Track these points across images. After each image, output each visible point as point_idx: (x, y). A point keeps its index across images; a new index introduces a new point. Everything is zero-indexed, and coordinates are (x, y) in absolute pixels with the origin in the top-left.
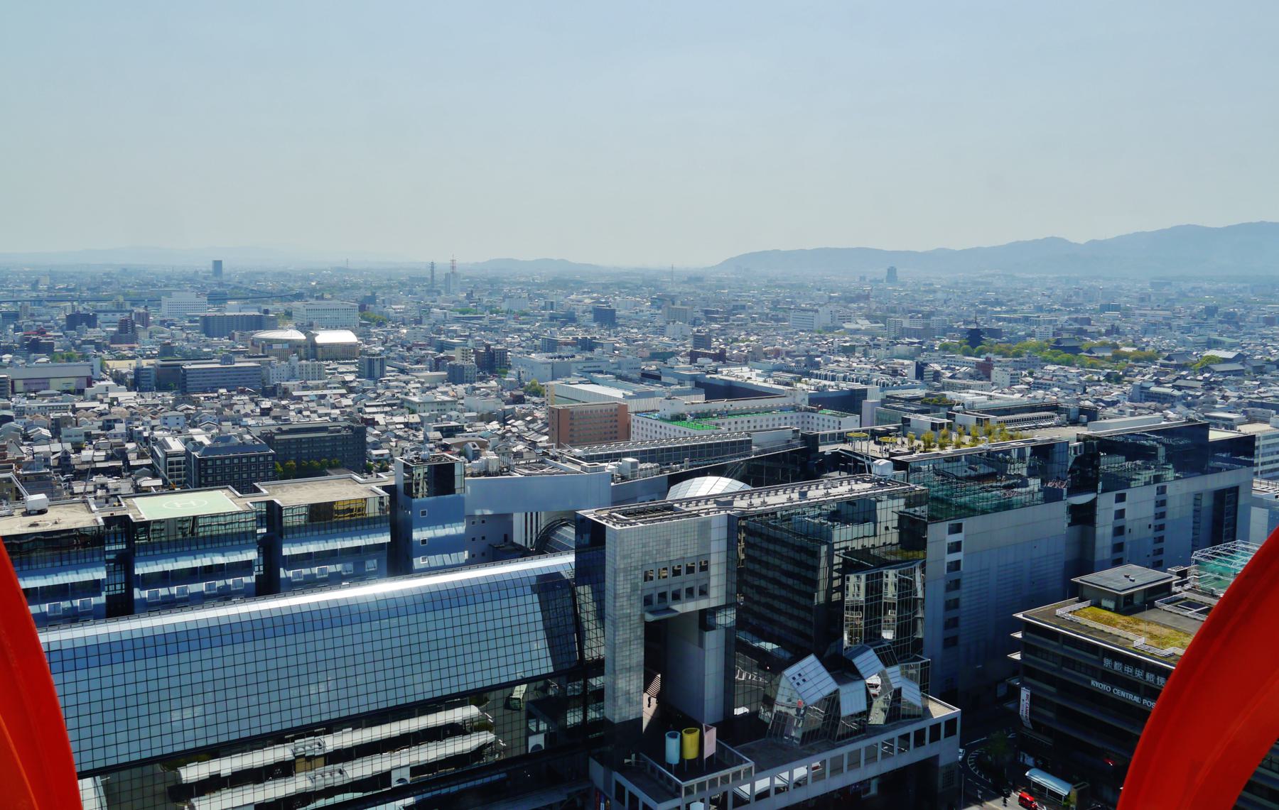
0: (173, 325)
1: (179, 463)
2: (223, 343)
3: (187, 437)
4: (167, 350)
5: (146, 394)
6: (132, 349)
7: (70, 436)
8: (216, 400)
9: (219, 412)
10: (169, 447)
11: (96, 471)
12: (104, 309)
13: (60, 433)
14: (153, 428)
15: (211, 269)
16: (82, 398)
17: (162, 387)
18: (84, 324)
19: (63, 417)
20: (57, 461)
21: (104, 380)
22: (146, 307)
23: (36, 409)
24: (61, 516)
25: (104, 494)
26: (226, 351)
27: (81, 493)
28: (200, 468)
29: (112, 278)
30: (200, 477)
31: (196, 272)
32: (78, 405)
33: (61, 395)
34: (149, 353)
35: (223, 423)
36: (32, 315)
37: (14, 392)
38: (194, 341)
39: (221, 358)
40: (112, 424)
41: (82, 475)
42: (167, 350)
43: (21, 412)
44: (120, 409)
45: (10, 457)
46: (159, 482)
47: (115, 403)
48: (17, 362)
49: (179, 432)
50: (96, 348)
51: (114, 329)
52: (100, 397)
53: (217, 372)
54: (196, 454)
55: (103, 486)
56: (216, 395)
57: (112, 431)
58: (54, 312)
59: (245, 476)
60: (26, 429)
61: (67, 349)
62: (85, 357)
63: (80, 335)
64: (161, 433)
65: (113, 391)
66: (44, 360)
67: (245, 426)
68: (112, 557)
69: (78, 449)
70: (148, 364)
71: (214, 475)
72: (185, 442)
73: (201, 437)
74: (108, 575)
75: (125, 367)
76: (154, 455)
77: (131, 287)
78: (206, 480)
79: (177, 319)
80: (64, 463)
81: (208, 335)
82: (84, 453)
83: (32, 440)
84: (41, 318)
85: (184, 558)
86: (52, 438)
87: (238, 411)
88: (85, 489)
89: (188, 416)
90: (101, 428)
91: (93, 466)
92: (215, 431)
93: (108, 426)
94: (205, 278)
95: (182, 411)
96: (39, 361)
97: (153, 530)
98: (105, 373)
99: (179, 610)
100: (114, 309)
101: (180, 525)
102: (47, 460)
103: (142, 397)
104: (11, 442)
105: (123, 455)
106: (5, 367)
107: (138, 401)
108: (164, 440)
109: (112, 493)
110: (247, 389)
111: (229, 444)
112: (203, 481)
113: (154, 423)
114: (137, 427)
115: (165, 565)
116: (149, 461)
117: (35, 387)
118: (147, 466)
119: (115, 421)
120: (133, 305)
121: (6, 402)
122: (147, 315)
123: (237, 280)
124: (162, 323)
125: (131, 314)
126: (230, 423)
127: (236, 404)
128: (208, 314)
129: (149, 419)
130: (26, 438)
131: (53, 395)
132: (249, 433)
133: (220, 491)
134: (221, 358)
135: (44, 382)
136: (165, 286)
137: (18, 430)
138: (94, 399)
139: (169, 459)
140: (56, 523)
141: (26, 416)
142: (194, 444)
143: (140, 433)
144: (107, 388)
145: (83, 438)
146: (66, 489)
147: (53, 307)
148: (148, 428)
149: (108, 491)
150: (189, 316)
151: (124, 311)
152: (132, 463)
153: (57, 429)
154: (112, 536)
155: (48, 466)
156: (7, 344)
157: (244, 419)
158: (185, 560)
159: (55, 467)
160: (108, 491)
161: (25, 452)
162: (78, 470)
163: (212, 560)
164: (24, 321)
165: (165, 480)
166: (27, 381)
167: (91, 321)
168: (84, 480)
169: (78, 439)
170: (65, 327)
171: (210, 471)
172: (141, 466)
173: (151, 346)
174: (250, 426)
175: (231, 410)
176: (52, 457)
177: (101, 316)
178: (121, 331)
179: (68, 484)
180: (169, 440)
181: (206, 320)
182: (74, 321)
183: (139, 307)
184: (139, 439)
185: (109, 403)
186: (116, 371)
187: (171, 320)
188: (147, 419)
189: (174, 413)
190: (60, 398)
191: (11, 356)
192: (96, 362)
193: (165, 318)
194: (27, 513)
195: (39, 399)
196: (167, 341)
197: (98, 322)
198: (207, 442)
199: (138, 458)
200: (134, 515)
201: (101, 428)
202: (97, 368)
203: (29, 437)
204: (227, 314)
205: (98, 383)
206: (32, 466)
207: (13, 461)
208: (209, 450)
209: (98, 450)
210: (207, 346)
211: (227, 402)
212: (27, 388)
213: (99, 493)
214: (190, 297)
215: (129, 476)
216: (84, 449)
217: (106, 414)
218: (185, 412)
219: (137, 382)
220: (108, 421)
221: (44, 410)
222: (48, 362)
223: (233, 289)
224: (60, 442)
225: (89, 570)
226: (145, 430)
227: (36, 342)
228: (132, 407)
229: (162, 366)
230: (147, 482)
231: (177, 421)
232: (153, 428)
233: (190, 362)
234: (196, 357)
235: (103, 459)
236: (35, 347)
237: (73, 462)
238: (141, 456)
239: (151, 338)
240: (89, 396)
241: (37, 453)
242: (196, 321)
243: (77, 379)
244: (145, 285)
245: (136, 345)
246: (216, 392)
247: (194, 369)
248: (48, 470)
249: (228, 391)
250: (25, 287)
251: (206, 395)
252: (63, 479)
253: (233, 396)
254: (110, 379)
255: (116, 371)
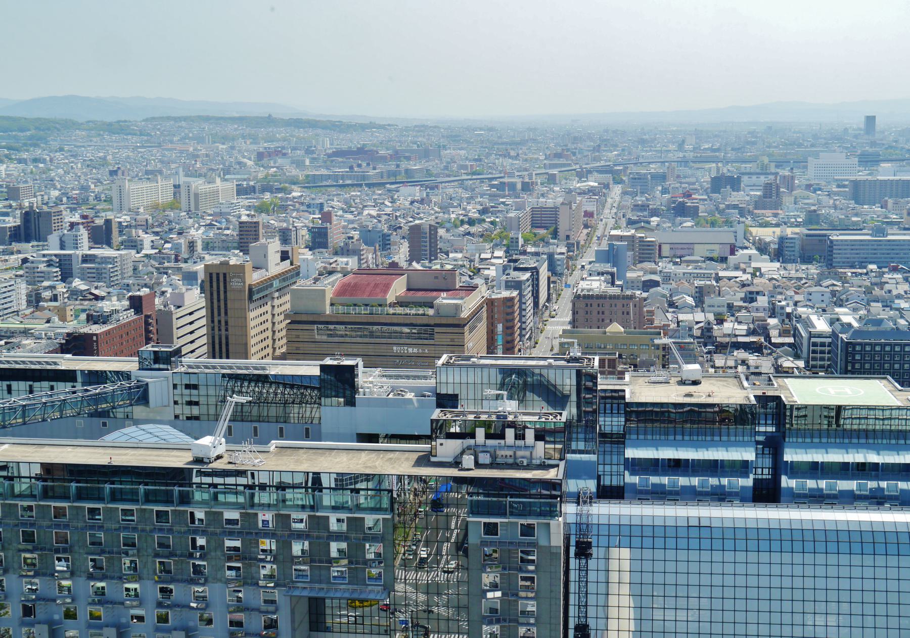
0: (820, 189)
1: (823, 345)
2: (874, 212)
3: (833, 316)
4: (812, 218)
5: (789, 266)
6: (775, 215)
7: (713, 306)
8: (864, 277)
9: (868, 291)
10: (814, 327)
11: (737, 346)
12: (748, 170)
13: (703, 302)
14: (796, 304)
15: (862, 126)
16: (725, 266)
17: (806, 259)
18: (728, 187)
19: (706, 285)
20: (700, 331)
21: (746, 248)
22: (792, 169)
23: (682, 275)
24: (714, 388)
25: (745, 370)
26: (878, 221)
27: (722, 368)
28: (847, 353)
29: (756, 137)
30: (847, 362)
31: (846, 130)
32: (721, 274)
33: (704, 262)
34: (793, 220)
35: (872, 304)
36: (678, 176)
37: (660, 257)
38: (841, 209)
39: (872, 229)
40: (754, 296)
41: (721, 348)
42: (812, 218)
43: (667, 278)
44: (763, 280)
45: (657, 323)
46: (801, 364)
47: (758, 274)
48: (664, 226)
49: (824, 310)
50: (739, 214)
51: (758, 193)
52: (743, 266)
53: (867, 245)
54: (844, 336)
55: (744, 362)
56: (865, 271)
57: (754, 304)
58: (699, 173)
59: (897, 366)
60: (671, 295)
61: (711, 213)
62: (728, 223)
63: (724, 199)
64: (805, 309)
65: (757, 261)
66: (689, 224)
67: (897, 309)
68: (761, 438)
69: (720, 321)
70: (793, 233)
71: (862, 362)
72: (832, 323)
73: (847, 317)
74: (756, 457)
75: (769, 235)
76: (796, 334)
77: (776, 147)
78: (853, 367)
79: (824, 183)
80: (707, 335)
81: (857, 203)
82: (726, 325)
83: (677, 307)
84: (687, 180)
85: (836, 450)
86: (696, 307)
87: (890, 291)
88: (725, 363)
89: (833, 293)
90: (744, 300)
91: (734, 340)
92: (863, 312)
93: (750, 298)
94: (856, 136)
95: (828, 287)
96: (685, 225)
97: (797, 417)
98: (748, 240)
99: (796, 506)
100: (758, 171)
101: (826, 414)
102: (690, 329)
103: (785, 269)
104: (658, 308)
105: (764, 331)
106: (652, 230)
107: (782, 273)
108: (808, 318)
109: (752, 370)
110: (901, 266)
111: (882, 328)
112: (849, 368)
113: (797, 298)
114: (780, 302)
115: (815, 455)
116: (791, 340)
117: (680, 254)
118: (789, 345)
119: (758, 293)
120: (777, 167)
121: (653, 265)
122: (793, 178)
123: (891, 138)
124: (808, 187)
125: (776, 177)
126: (880, 305)
127: (887, 283)
128: (859, 178)
129: (793, 293)
130: (672, 304)
131: (697, 262)
132: (902, 317)
133: (877, 381)
134: (872, 229)
135: (689, 247)
136: (812, 146)
137: (664, 296)
138: (737, 268)
139: (813, 340)
140: (709, 396)
141: (671, 281)
142: (842, 325)
143: (782, 308)
144: (750, 257)
145: (725, 309)
146: (707, 361)
147: (698, 169)
148: (791, 303)
149: (748, 368)
150: (837, 180)
151: (768, 174)
152: (773, 340)
153: (700, 296)
154: (763, 416)
155: (692, 336)
156: (655, 207)
157: (897, 301)
158: (837, 453)
159: (698, 338)
160: (748, 368)
161: (670, 319)
162: (719, 342)
163: (865, 457)
164: (671, 183)
165: (807, 362)
166: (672, 246)
167: (734, 183)
168: (725, 354)
169: (720, 310)
170: (709, 190)
171: (858, 357)
172: (783, 345)
173: (796, 213)
174: (903, 309)
175: (882, 289)
176: (696, 327)
177: (745, 179)
178: (765, 196)
179: (709, 356)
180: (814, 318)
181: (856, 184)
182: (719, 183)
183: (784, 169)
184: (782, 314)
185: (752, 274)
186: (760, 239)
187: (818, 184)
188: (790, 293)
189: (818, 288)
190: (703, 265)
191: (658, 219)
192: (740, 229)
193: (812, 182)
194: (682, 383)
195: (684, 265)
196: (813, 208)
197: (742, 185)
198: (856, 324)
199: (780, 336)
200: (786, 397)
201: (744, 300)
202: (740, 235)
203: (674, 304)
204: (880, 178)
205: (741, 252)
206: (677, 334)
207: (660, 328)
208: (858, 333)
209: (740, 323)
210: (856, 215)
211: (877, 280)
212: (673, 253)
213: (740, 369)
214: (839, 158)
215: (770, 354)
216: (726, 320)
217: (749, 285)
218: (831, 288)
219: (780, 252)
220: (751, 293)
221: (689, 277)
222: (692, 227)
223: (887, 149)
224: (703, 311)
225: (739, 449)
226: (788, 305)
227: (682, 204)
228: (775, 279)
229: (807, 235)
230: (787, 363)
231: (823, 298)
232: (796, 304)
233: (838, 232)
234: (845, 227)
235: (744, 333)
236: (681, 210)
237: (715, 333)
238: (783, 333)
239: (795, 203)
240: (732, 265)
241: (681, 321)
242: (844, 186)
243: (721, 246)
244: (791, 145)
245: (780, 212)
246: (865, 267)
247: (842, 240)
248: (692, 340)
249: (879, 267)
250: (672, 147)
251: (854, 270)
252: (705, 351)
253: (884, 273)
254: (753, 247)
255: (760, 239)
